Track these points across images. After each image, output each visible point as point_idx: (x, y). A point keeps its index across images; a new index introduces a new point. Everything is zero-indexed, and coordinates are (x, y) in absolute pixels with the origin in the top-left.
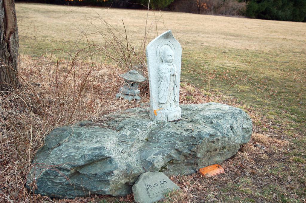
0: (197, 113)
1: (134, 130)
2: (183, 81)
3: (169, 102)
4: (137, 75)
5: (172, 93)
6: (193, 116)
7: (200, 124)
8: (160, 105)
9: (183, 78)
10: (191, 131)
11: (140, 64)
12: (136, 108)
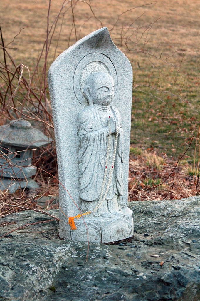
0: (171, 223)
1: (22, 267)
2: (139, 143)
3: (105, 197)
4: (29, 131)
5: (111, 176)
6: (161, 229)
7: (179, 250)
8: (84, 206)
9: (138, 134)
10: (157, 266)
11: (37, 104)
12: (27, 212)
